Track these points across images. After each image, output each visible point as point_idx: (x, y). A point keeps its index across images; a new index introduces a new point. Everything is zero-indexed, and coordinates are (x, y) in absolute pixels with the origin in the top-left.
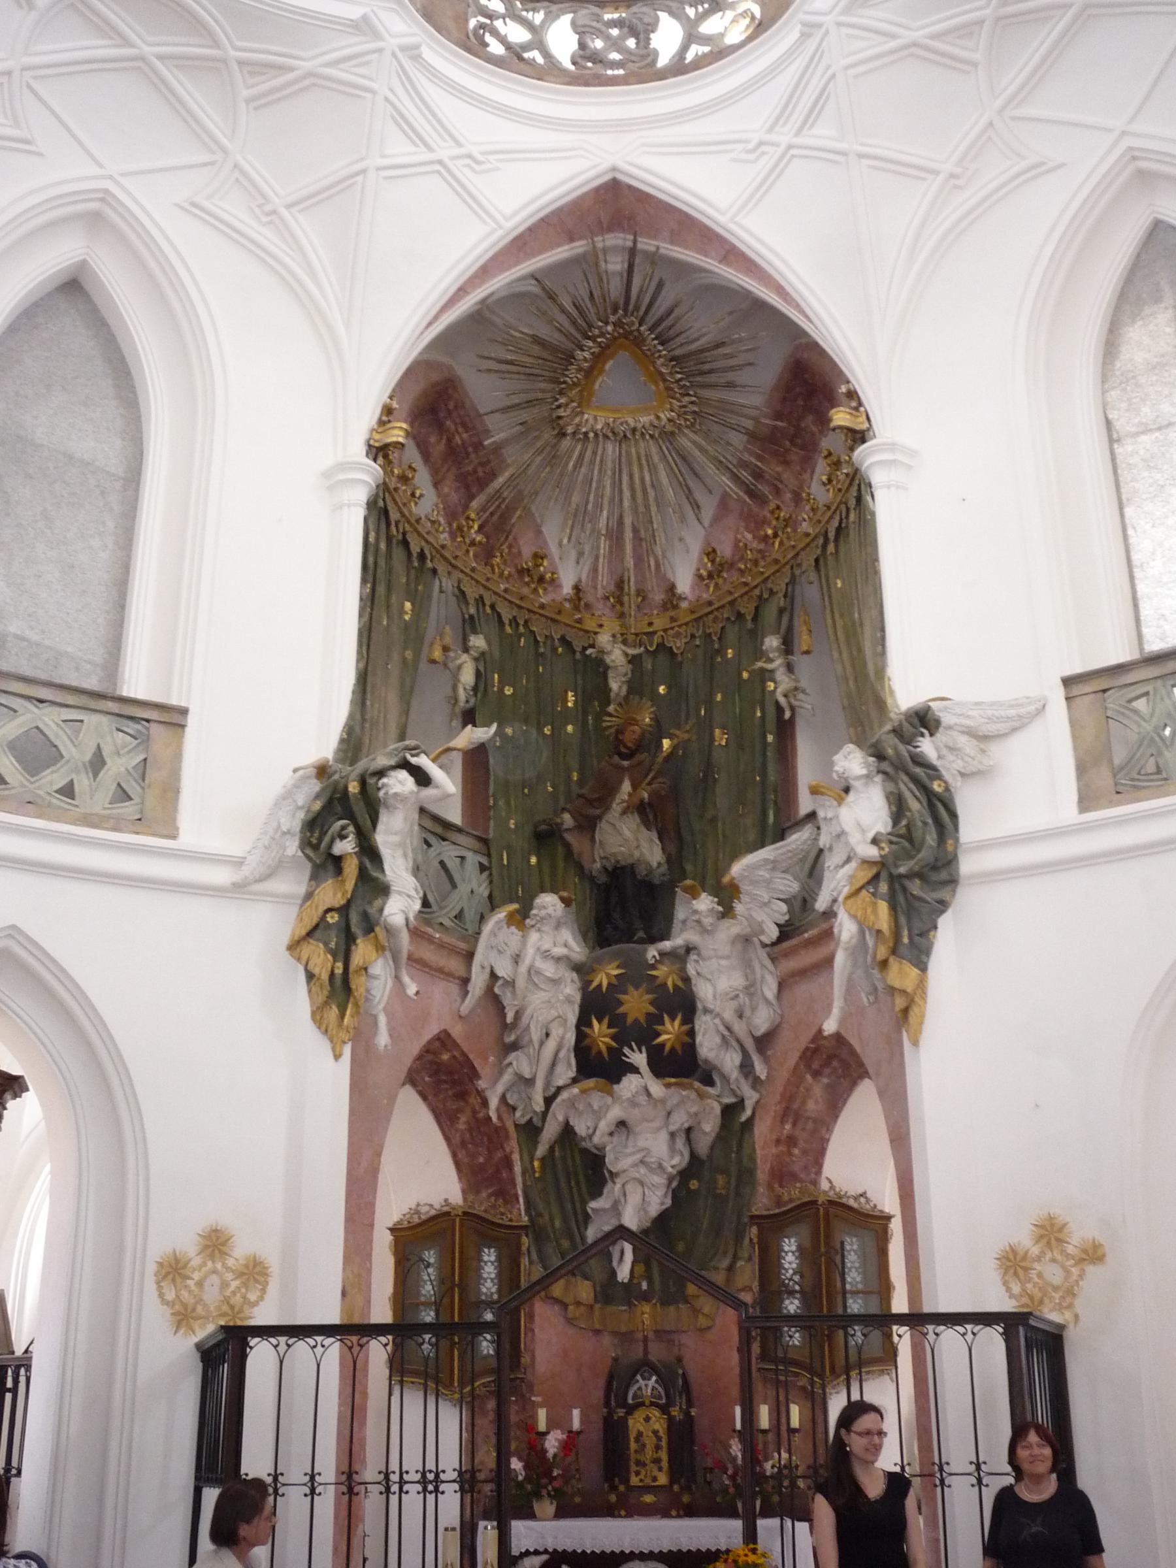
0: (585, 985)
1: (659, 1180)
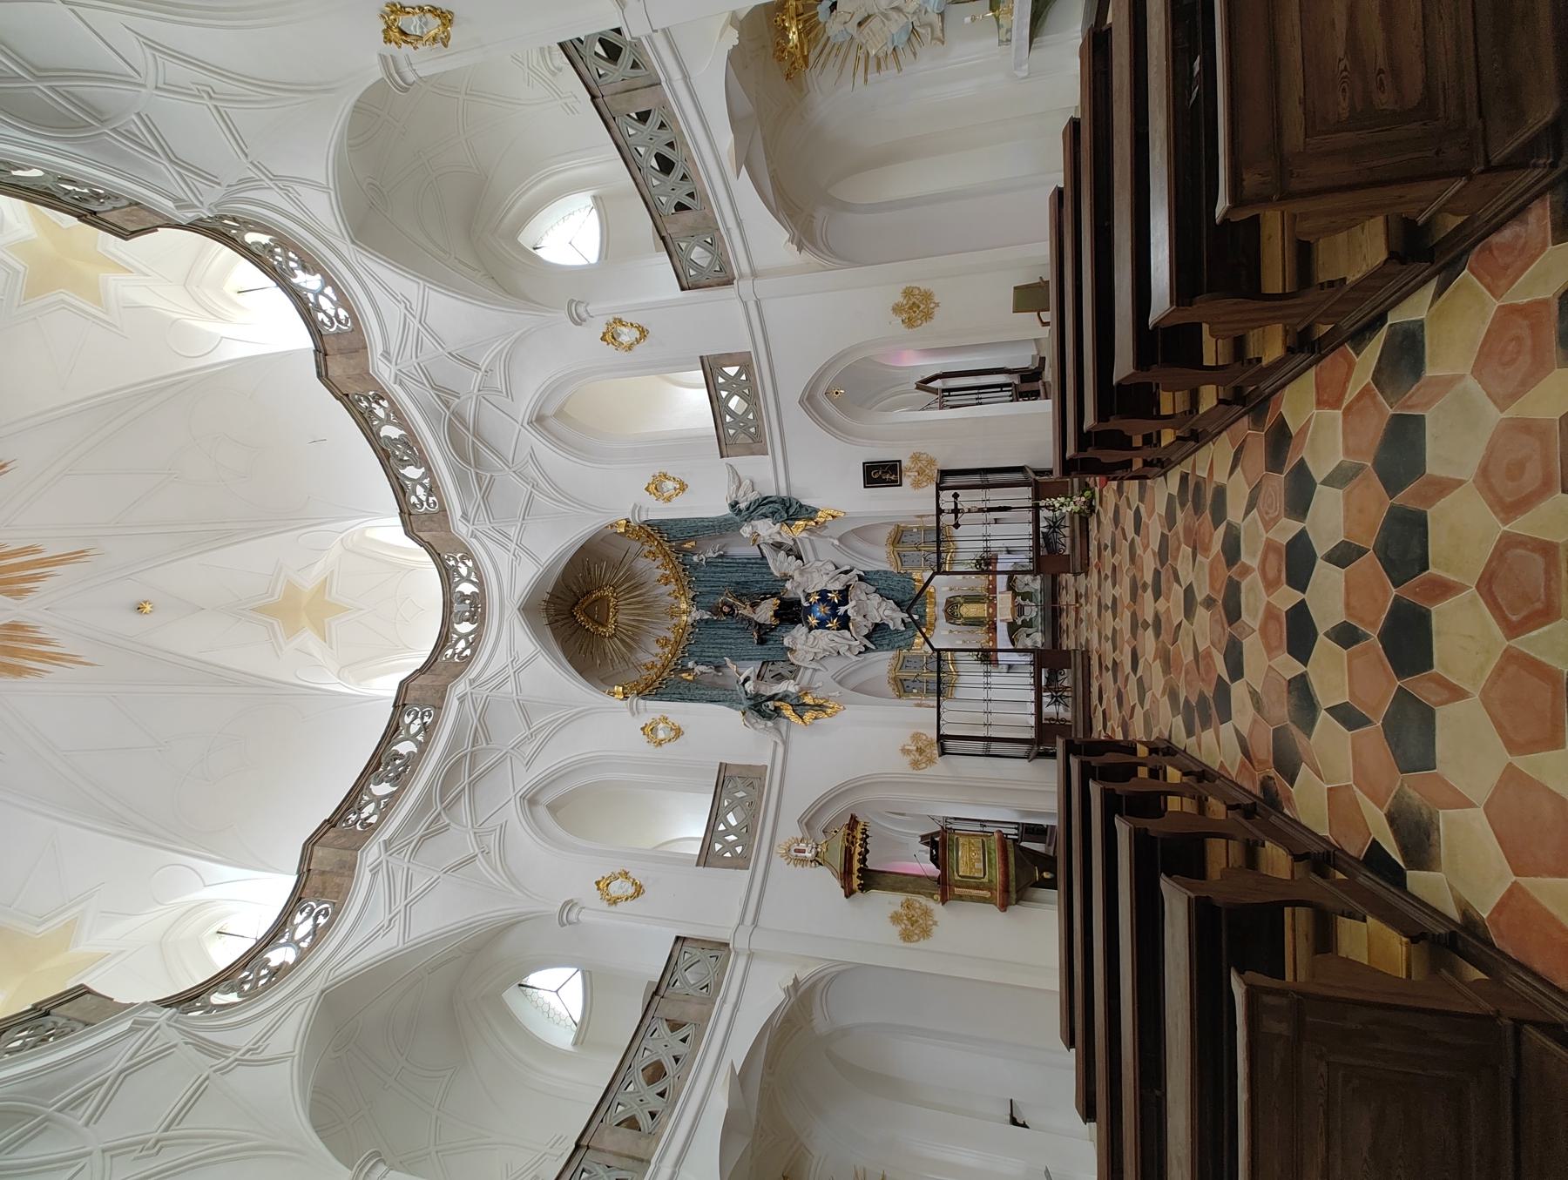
0: (816, 628)
1: (884, 604)
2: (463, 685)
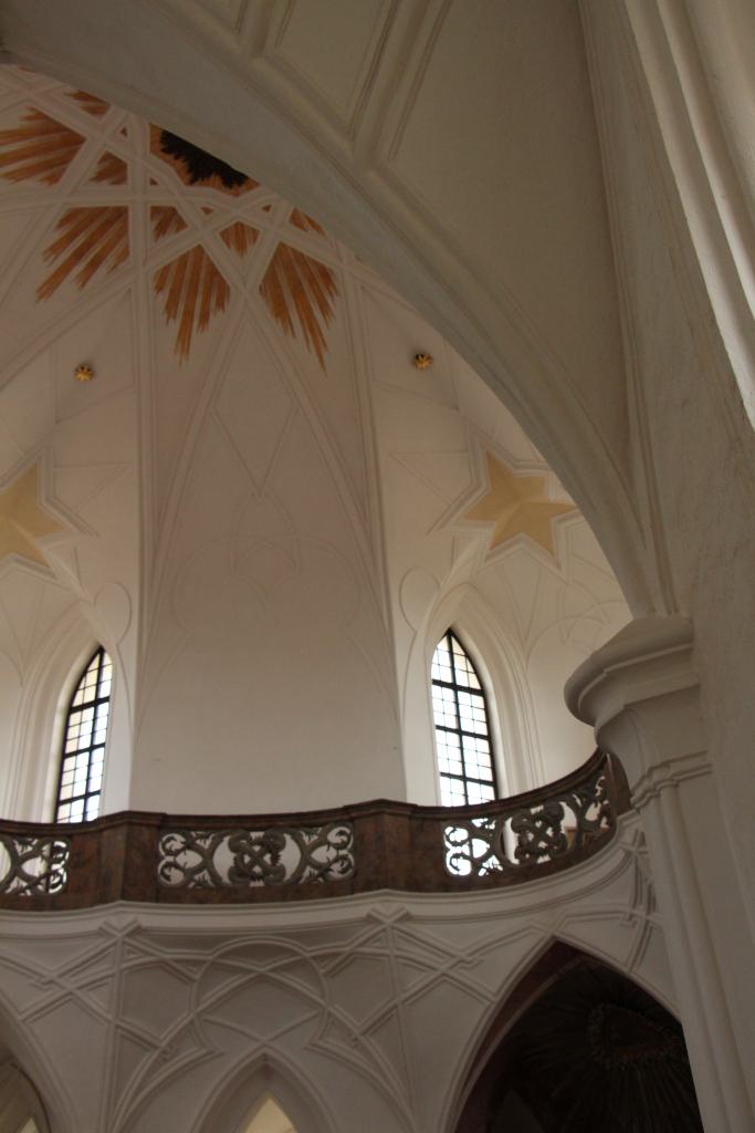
2: (395, 907)
